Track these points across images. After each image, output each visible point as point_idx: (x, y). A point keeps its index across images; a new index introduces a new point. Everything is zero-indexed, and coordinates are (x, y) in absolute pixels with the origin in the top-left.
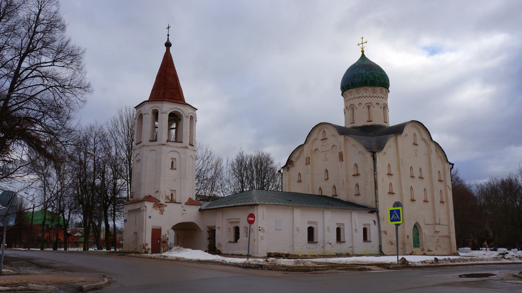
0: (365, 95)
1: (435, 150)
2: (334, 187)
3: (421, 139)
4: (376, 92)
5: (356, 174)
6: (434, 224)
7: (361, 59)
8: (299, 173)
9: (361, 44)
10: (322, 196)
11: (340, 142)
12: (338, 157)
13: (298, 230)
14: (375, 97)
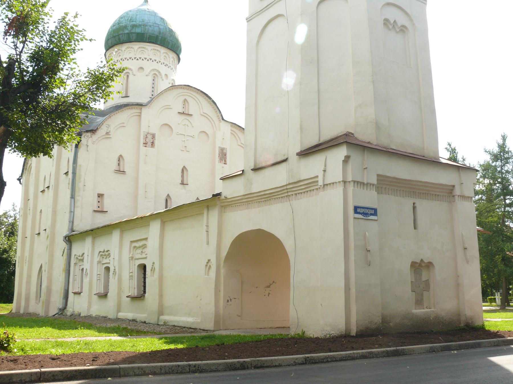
8: (120, 158)
12: (217, 155)
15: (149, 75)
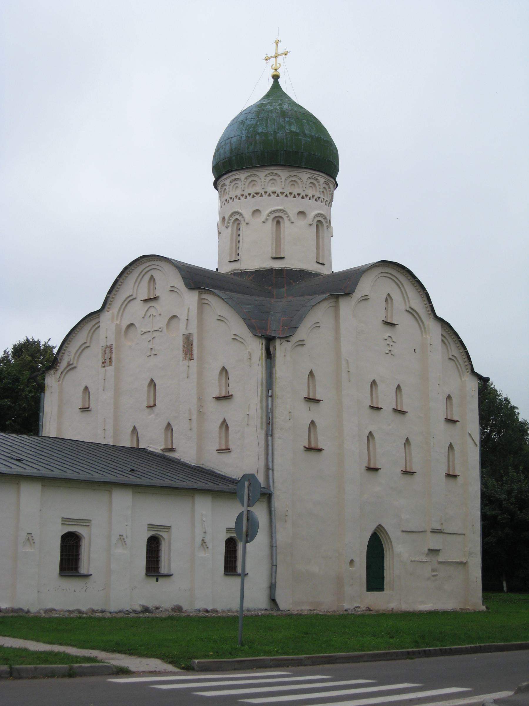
0: (270, 189)
1: (442, 341)
2: (169, 427)
3: (407, 311)
4: (299, 181)
5: (223, 394)
6: (425, 531)
7: (268, 95)
8: (86, 388)
9: (272, 57)
10: (138, 449)
11: (189, 309)
13: (30, 539)
14: (297, 196)
15: (229, 226)
